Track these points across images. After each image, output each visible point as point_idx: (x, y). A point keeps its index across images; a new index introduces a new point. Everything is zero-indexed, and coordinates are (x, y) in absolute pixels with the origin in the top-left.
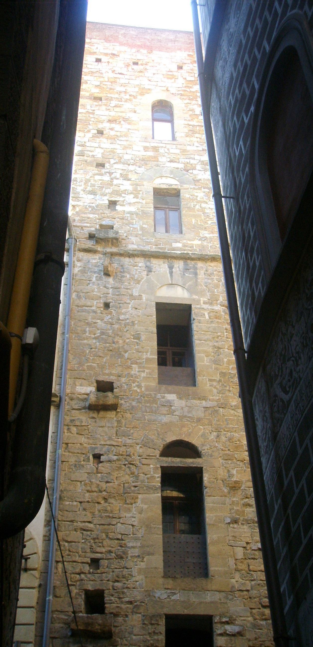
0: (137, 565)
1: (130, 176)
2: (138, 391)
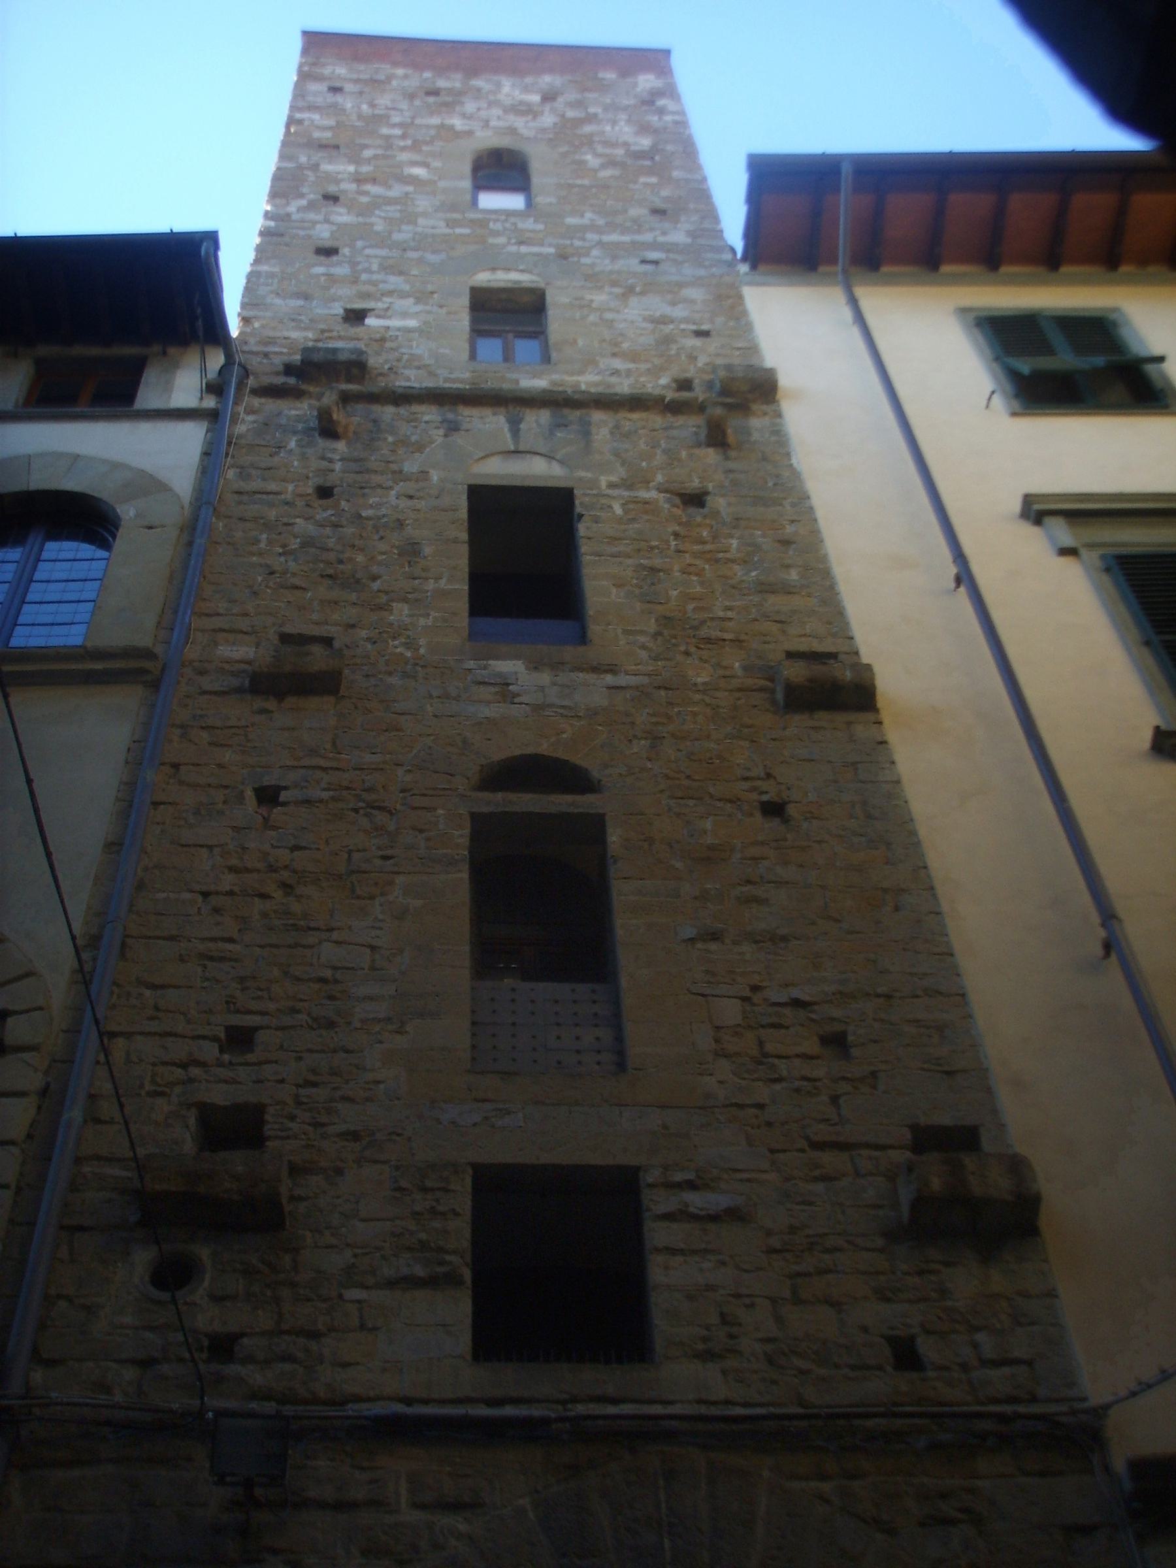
0: (381, 1042)
2: (409, 654)
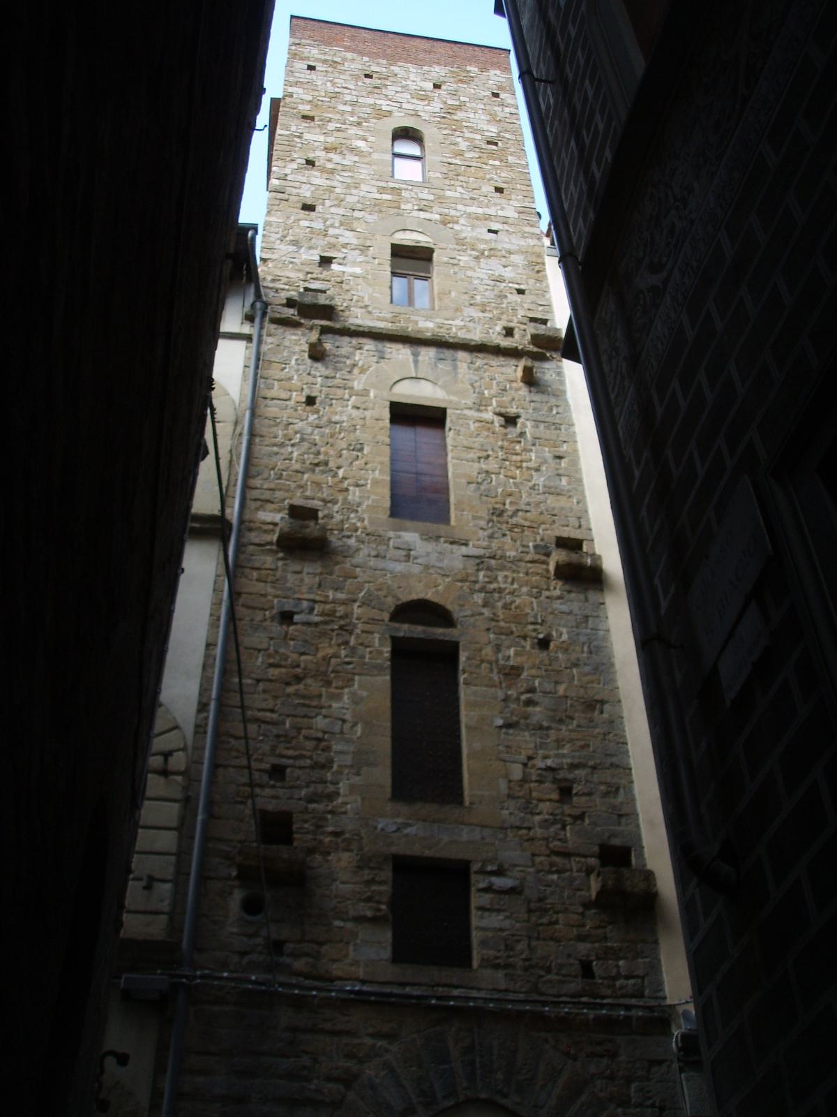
1: (355, 225)
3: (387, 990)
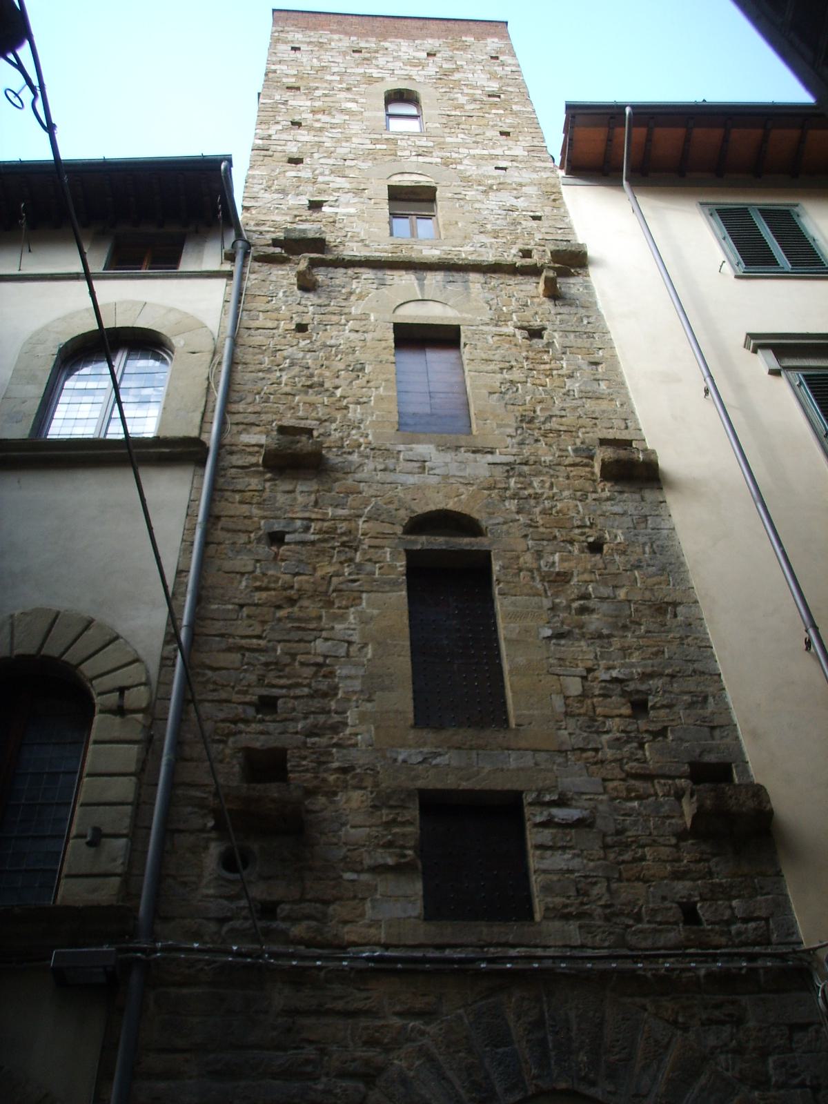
1: (347, 172)
3: (418, 954)
